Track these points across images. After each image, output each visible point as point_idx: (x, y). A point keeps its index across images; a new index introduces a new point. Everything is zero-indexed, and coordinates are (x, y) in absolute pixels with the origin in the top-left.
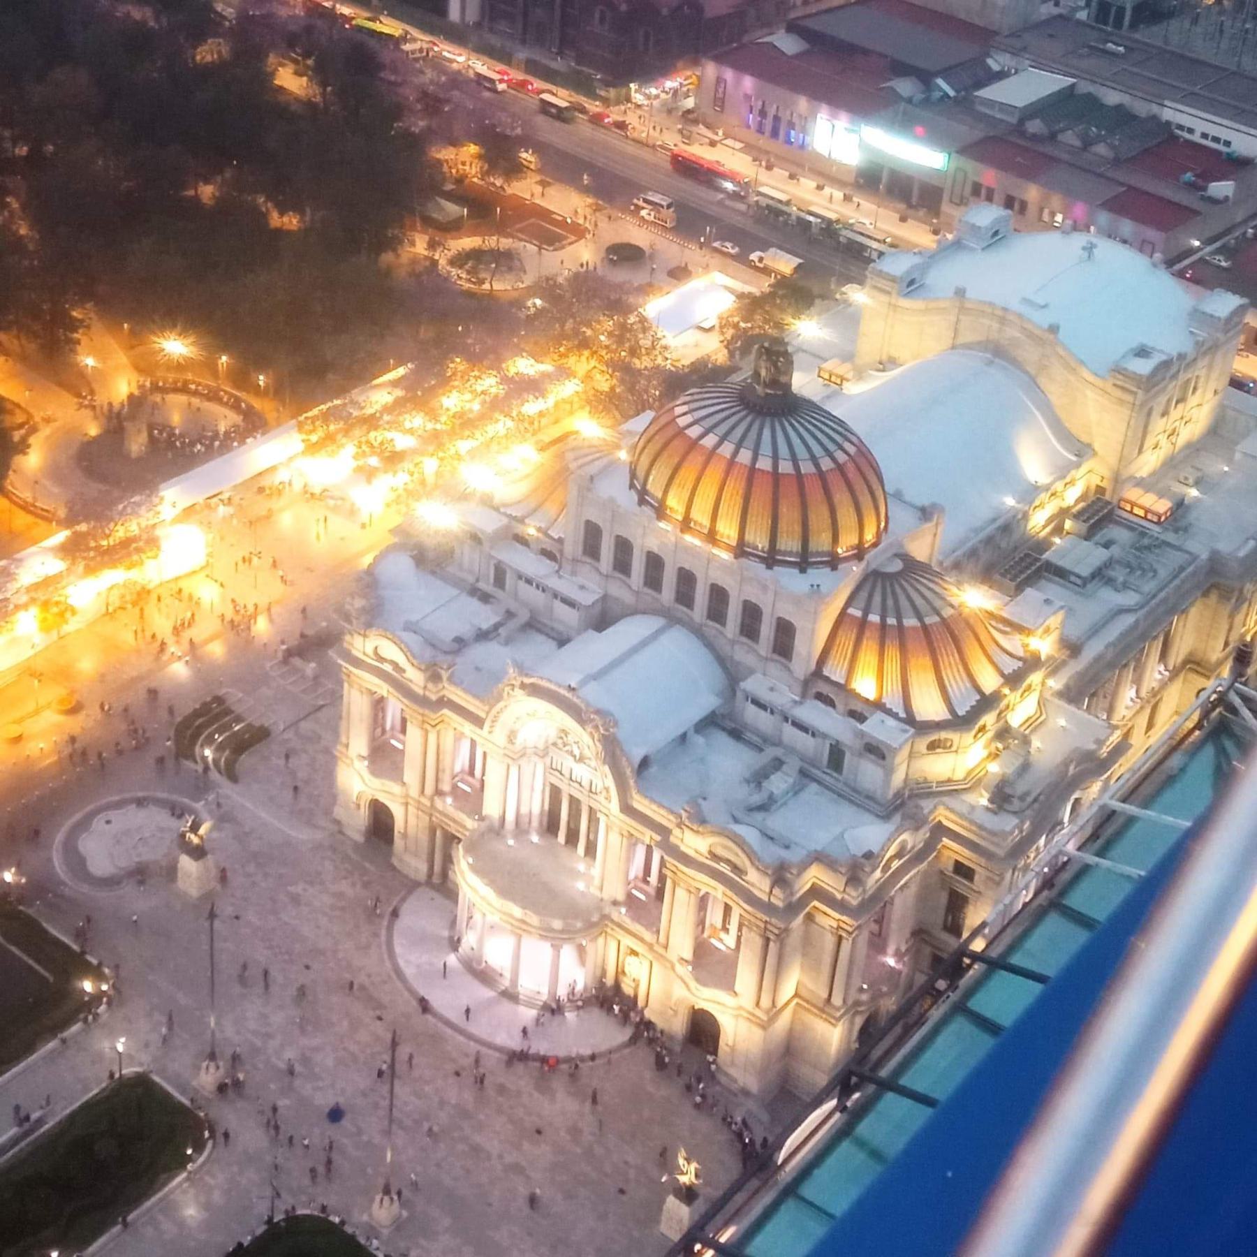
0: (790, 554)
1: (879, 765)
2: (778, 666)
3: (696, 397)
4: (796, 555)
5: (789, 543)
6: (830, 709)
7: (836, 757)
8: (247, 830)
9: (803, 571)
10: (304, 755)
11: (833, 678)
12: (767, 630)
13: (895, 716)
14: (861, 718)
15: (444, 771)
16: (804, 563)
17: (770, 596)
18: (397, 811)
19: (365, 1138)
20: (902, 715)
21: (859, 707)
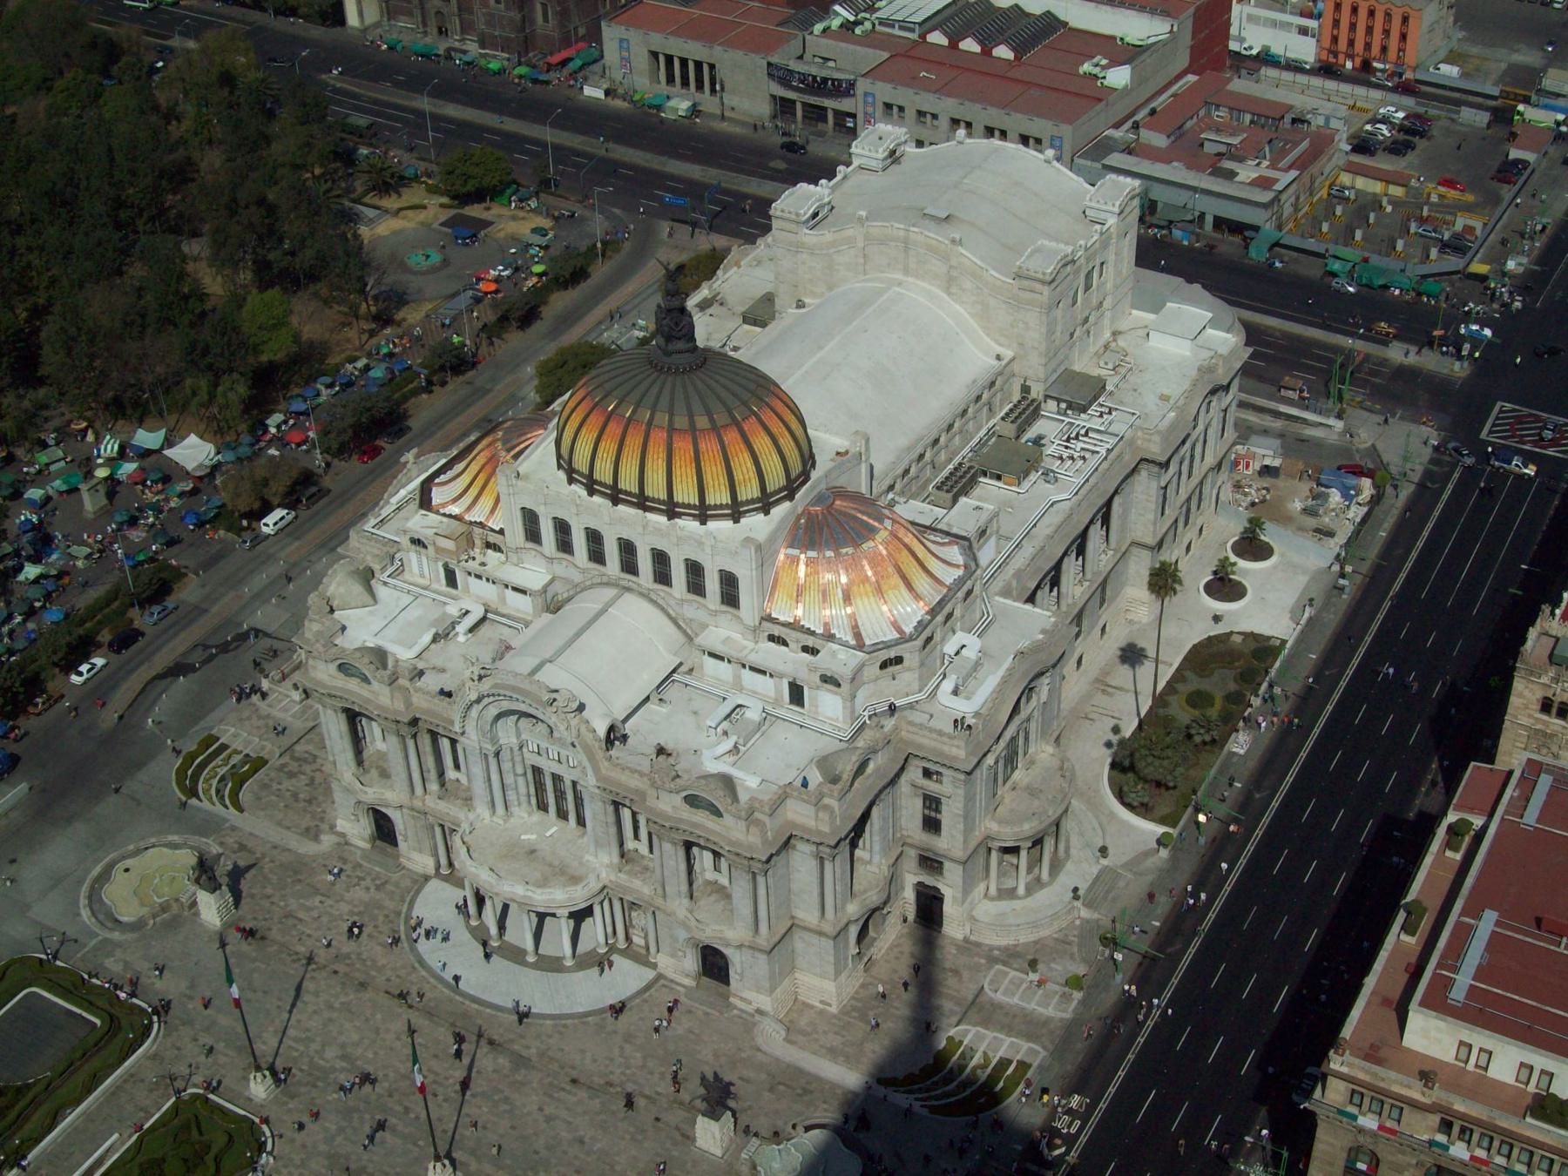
0: (721, 507)
1: (836, 693)
2: (729, 617)
3: (605, 369)
4: (727, 506)
5: (718, 495)
6: (783, 648)
7: (797, 694)
8: (258, 855)
9: (736, 521)
10: (303, 777)
11: (782, 618)
12: (712, 584)
13: (845, 645)
14: (813, 651)
15: (429, 771)
16: (736, 512)
17: (708, 550)
18: (395, 816)
19: (412, 1116)
20: (853, 642)
21: (810, 641)
